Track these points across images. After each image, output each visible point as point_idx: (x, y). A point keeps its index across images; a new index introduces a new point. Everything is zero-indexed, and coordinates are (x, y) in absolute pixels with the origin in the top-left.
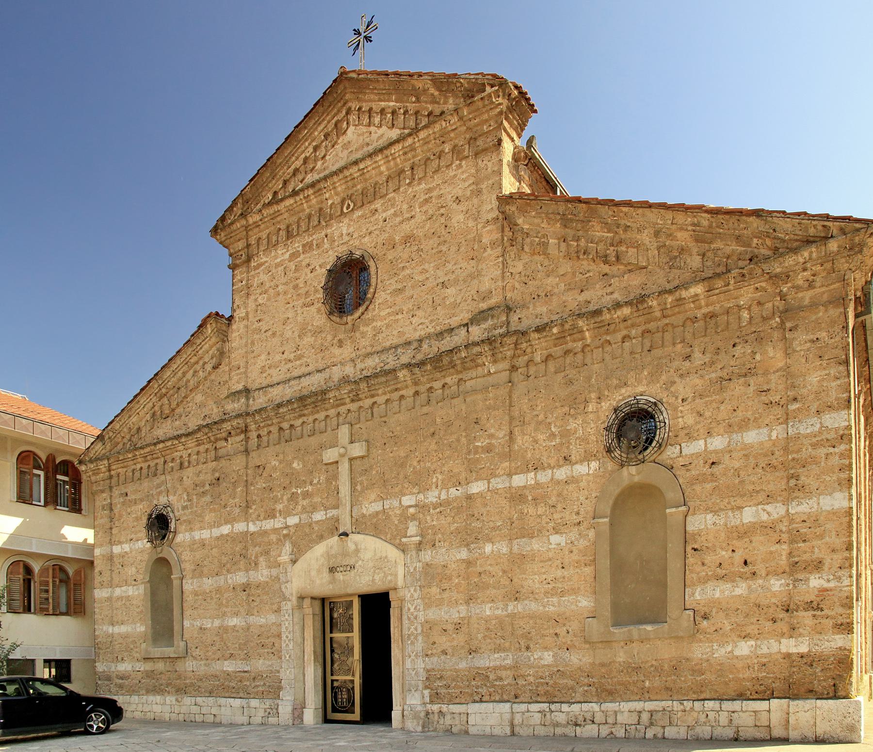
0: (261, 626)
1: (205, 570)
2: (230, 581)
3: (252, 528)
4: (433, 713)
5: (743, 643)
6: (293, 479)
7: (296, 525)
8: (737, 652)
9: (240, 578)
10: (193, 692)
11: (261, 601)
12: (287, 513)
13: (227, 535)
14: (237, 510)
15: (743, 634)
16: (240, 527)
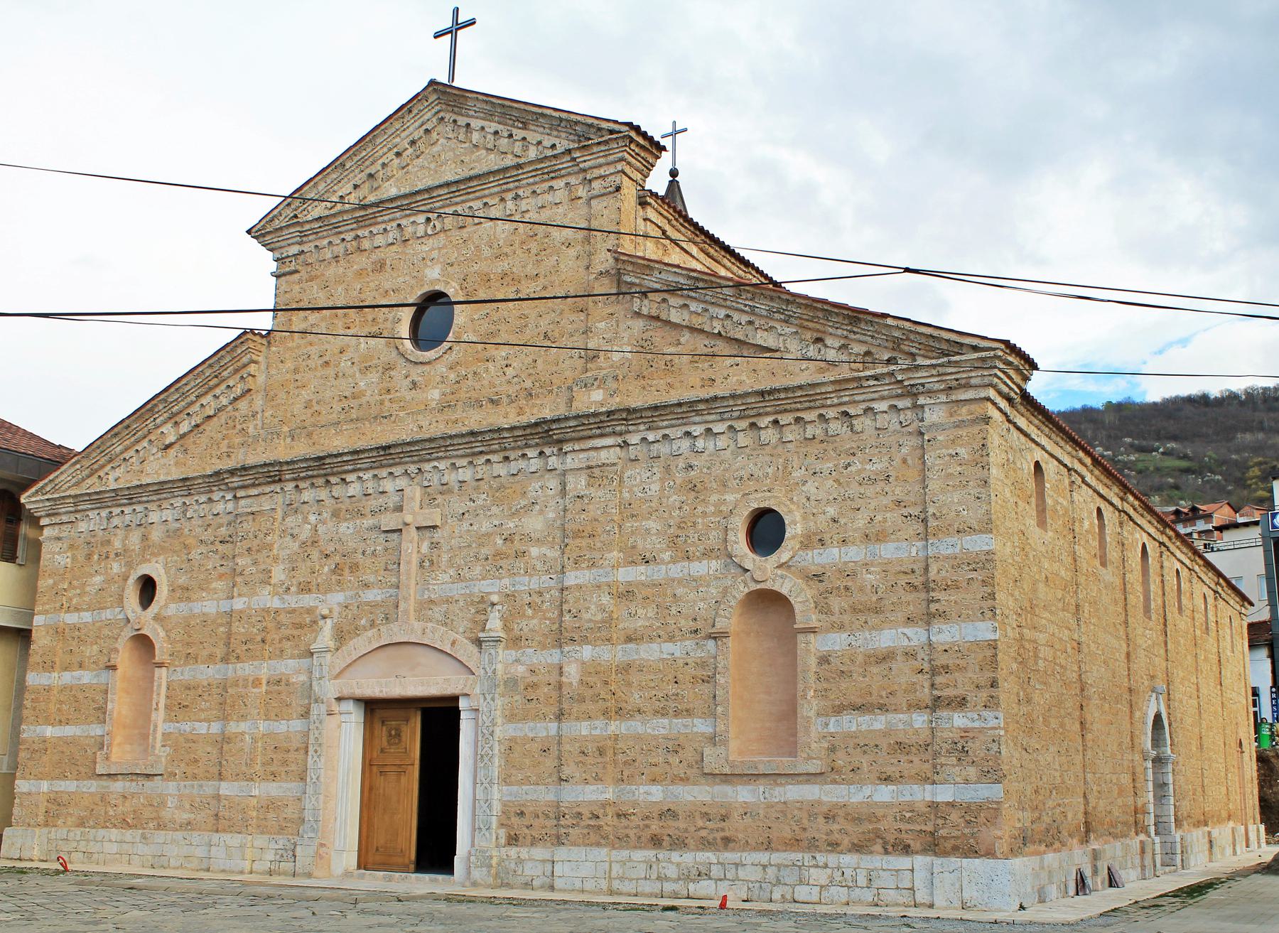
5: (884, 786)
13: (241, 612)
15: (884, 776)
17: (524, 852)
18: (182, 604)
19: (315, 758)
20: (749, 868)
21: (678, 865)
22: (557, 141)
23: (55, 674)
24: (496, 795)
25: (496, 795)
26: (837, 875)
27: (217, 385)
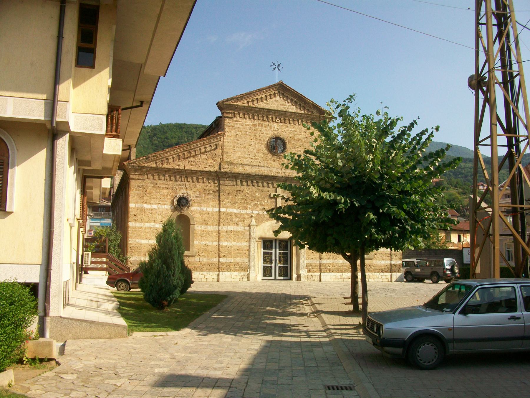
0: (239, 246)
1: (209, 223)
2: (224, 229)
3: (235, 211)
4: (309, 276)
6: (255, 198)
7: (257, 214)
9: (230, 228)
10: (199, 270)
11: (239, 238)
12: (252, 209)
13: (224, 212)
14: (229, 204)
16: (230, 210)
17: (313, 274)
22: (313, 111)
23: (143, 224)
24: (305, 262)
25: (305, 262)
27: (207, 145)
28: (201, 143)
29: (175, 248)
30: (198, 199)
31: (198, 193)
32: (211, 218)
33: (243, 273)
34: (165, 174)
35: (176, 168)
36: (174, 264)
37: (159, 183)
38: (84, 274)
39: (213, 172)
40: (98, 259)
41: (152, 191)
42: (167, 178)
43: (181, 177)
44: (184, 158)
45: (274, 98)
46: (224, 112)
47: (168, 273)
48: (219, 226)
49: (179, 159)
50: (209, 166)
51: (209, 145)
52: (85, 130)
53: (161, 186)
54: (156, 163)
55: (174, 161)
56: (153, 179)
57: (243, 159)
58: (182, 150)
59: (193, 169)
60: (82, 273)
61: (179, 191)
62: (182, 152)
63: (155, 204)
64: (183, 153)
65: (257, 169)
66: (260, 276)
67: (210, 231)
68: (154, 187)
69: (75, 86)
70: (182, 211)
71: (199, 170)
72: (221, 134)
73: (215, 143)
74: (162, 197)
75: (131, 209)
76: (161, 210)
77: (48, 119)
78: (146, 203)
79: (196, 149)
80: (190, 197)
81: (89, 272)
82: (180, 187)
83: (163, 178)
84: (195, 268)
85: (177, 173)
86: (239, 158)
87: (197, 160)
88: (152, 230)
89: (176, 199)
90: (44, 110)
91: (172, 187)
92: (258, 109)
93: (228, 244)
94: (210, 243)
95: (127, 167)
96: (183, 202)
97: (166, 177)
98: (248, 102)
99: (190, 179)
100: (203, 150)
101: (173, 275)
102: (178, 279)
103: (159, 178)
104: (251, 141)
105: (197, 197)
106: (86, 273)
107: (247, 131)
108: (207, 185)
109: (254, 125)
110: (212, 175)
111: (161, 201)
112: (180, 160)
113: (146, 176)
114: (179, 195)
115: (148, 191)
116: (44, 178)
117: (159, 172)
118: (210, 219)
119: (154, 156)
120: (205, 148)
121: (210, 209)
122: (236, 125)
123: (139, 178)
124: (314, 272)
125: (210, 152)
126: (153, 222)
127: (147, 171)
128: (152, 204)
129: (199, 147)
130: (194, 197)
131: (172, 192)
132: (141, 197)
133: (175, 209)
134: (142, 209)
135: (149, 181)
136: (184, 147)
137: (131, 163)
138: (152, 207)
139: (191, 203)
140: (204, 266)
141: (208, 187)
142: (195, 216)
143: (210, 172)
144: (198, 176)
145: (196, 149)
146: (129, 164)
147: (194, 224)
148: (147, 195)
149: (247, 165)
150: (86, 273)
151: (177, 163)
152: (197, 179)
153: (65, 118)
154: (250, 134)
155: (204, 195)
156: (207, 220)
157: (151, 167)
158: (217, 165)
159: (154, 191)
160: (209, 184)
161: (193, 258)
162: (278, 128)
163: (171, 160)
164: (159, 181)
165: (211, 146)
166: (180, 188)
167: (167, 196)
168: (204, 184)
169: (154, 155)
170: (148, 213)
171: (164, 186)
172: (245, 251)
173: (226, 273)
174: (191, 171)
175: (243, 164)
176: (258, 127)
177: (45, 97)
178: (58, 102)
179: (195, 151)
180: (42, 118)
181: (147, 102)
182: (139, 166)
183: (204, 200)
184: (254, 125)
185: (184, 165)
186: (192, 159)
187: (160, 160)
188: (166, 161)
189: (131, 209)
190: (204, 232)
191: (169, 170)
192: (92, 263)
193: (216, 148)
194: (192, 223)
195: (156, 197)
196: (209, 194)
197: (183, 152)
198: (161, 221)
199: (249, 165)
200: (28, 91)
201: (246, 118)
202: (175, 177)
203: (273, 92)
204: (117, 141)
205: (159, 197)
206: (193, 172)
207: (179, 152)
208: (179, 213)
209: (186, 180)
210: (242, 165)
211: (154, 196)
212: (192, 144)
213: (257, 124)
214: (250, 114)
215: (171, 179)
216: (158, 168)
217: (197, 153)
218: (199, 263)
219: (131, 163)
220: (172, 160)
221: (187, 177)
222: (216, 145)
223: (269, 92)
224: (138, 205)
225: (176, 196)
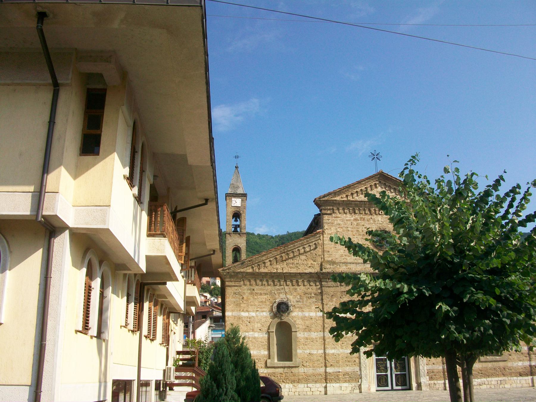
4: (431, 384)
8: (519, 365)
10: (304, 382)
17: (436, 382)
18: (299, 313)
19: (364, 360)
20: (494, 382)
21: (477, 382)
25: (426, 368)
26: (513, 381)
27: (306, 245)
28: (299, 243)
29: (227, 361)
30: (300, 303)
31: (299, 298)
32: (314, 324)
33: (353, 384)
34: (262, 279)
35: (274, 272)
36: (225, 380)
37: (257, 289)
38: (169, 390)
39: (313, 273)
40: (183, 374)
41: (249, 297)
42: (265, 283)
43: (279, 281)
44: (282, 261)
45: (375, 189)
46: (322, 209)
47: (219, 391)
48: (324, 332)
49: (277, 262)
50: (310, 267)
51: (308, 245)
52: (87, 224)
53: (259, 292)
54: (253, 268)
55: (271, 264)
56: (250, 285)
57: (346, 257)
58: (279, 252)
59: (291, 272)
60: (166, 389)
61: (278, 296)
62: (279, 255)
63: (253, 311)
64: (280, 255)
65: (362, 267)
66: (374, 387)
67: (314, 338)
68: (251, 294)
69: (75, 176)
70: (282, 318)
71: (299, 272)
72: (319, 232)
73: (314, 243)
74: (260, 304)
75: (228, 318)
76: (259, 317)
77: (35, 213)
78: (243, 311)
79: (294, 250)
80: (290, 302)
81: (175, 388)
82: (279, 291)
83: (260, 283)
84: (299, 380)
85: (275, 277)
86: (342, 256)
87: (296, 262)
88: (250, 339)
89: (275, 305)
90: (30, 204)
91: (271, 293)
92: (358, 203)
93: (335, 352)
94: (315, 352)
95: (222, 274)
96: (283, 308)
97: (263, 282)
98: (347, 196)
99: (289, 282)
100: (302, 251)
101: (226, 394)
102: (232, 399)
103: (256, 283)
104: (354, 237)
105: (297, 301)
106: (171, 389)
107: (348, 226)
108: (309, 288)
109: (356, 220)
110: (313, 277)
111: (259, 308)
112: (278, 263)
113: (242, 282)
114: (277, 301)
115: (245, 298)
116: (38, 283)
117: (256, 277)
118: (313, 325)
119: (249, 261)
120: (304, 248)
121: (313, 314)
122: (336, 222)
123: (235, 285)
124: (437, 380)
125: (309, 253)
126: (251, 330)
127: (243, 277)
128: (250, 311)
129: (297, 248)
130: (295, 301)
131: (271, 298)
132: (238, 305)
133: (275, 316)
134: (239, 318)
135: (245, 288)
136: (281, 249)
137: (226, 270)
138: (250, 315)
139: (291, 308)
140: (309, 378)
141: (310, 290)
142: (297, 322)
143: (311, 273)
144: (297, 279)
145: (294, 250)
146: (223, 270)
147: (296, 332)
148: (245, 302)
149: (350, 263)
150: (171, 389)
151: (275, 267)
152: (297, 282)
153: (53, 211)
154: (352, 230)
155: (305, 299)
156: (310, 326)
157: (247, 273)
158: (318, 266)
159: (251, 298)
160: (311, 287)
161: (297, 368)
162: (382, 220)
163: (268, 264)
164: (257, 287)
165: (310, 246)
166: (280, 293)
167: (265, 302)
168: (304, 287)
169: (250, 259)
170: (246, 322)
171: (262, 292)
172: (354, 359)
173: (334, 385)
174: (289, 274)
175: (347, 263)
176: (360, 221)
177: (32, 188)
178: (46, 194)
179: (293, 252)
180: (28, 213)
181: (213, 199)
182: (234, 273)
183: (305, 304)
184: (356, 220)
185: (283, 268)
186: (290, 261)
187: (256, 265)
188: (263, 265)
189: (228, 318)
190: (307, 339)
191: (266, 274)
192: (177, 378)
193: (316, 248)
194: (294, 330)
195: (253, 303)
196: (311, 297)
197: (280, 254)
198: (260, 330)
199: (353, 263)
200: (14, 184)
201: (346, 213)
202: (273, 282)
203: (374, 183)
204: (161, 240)
205: (257, 303)
206: (292, 274)
207: (276, 254)
208: (279, 319)
209: (285, 284)
210: (346, 263)
211: (252, 303)
212: (289, 245)
213: (359, 218)
214: (350, 208)
215: (269, 284)
216: (254, 273)
217: (295, 255)
218: (303, 374)
219: (226, 270)
220: (269, 263)
221: (285, 281)
222: (315, 244)
223: (368, 183)
224: (235, 313)
225: (275, 302)
